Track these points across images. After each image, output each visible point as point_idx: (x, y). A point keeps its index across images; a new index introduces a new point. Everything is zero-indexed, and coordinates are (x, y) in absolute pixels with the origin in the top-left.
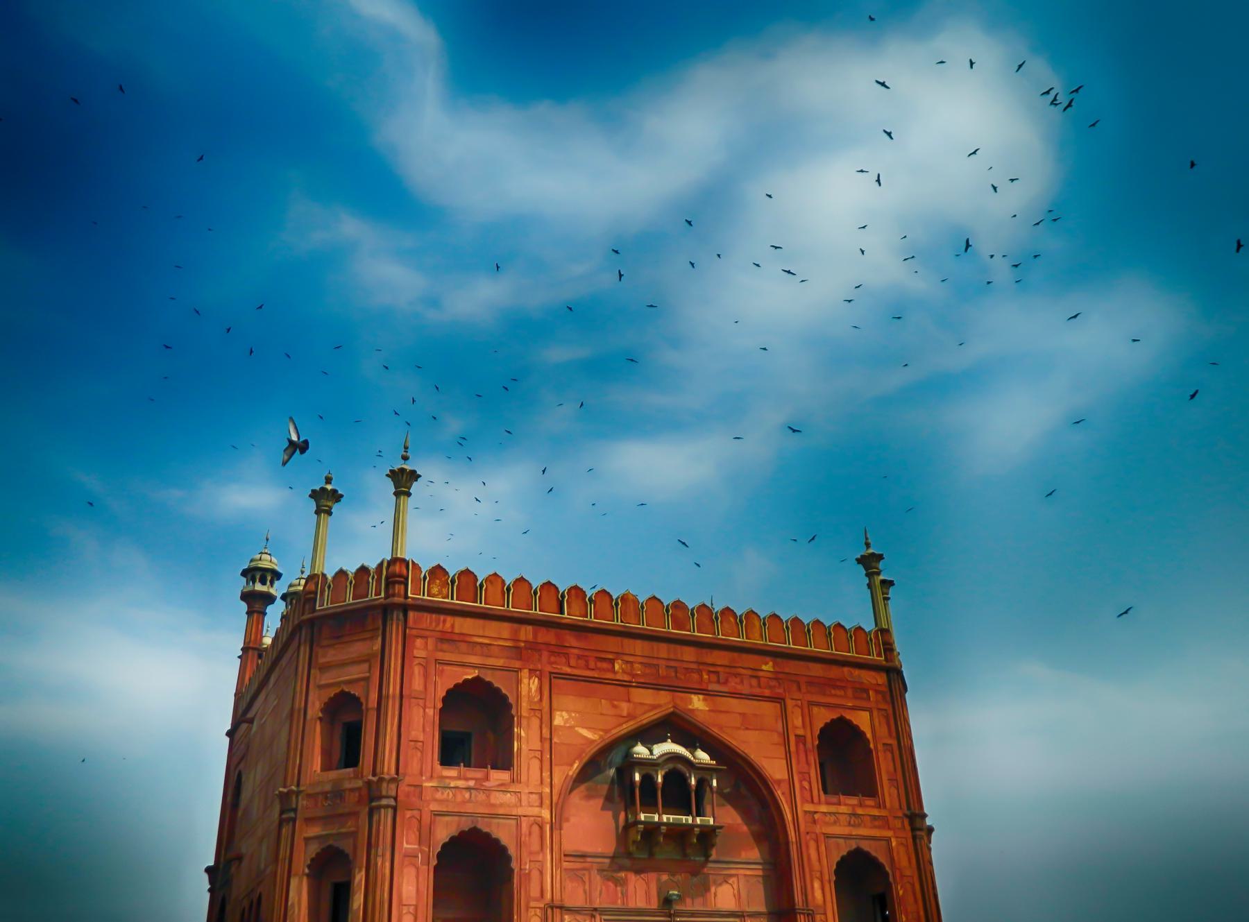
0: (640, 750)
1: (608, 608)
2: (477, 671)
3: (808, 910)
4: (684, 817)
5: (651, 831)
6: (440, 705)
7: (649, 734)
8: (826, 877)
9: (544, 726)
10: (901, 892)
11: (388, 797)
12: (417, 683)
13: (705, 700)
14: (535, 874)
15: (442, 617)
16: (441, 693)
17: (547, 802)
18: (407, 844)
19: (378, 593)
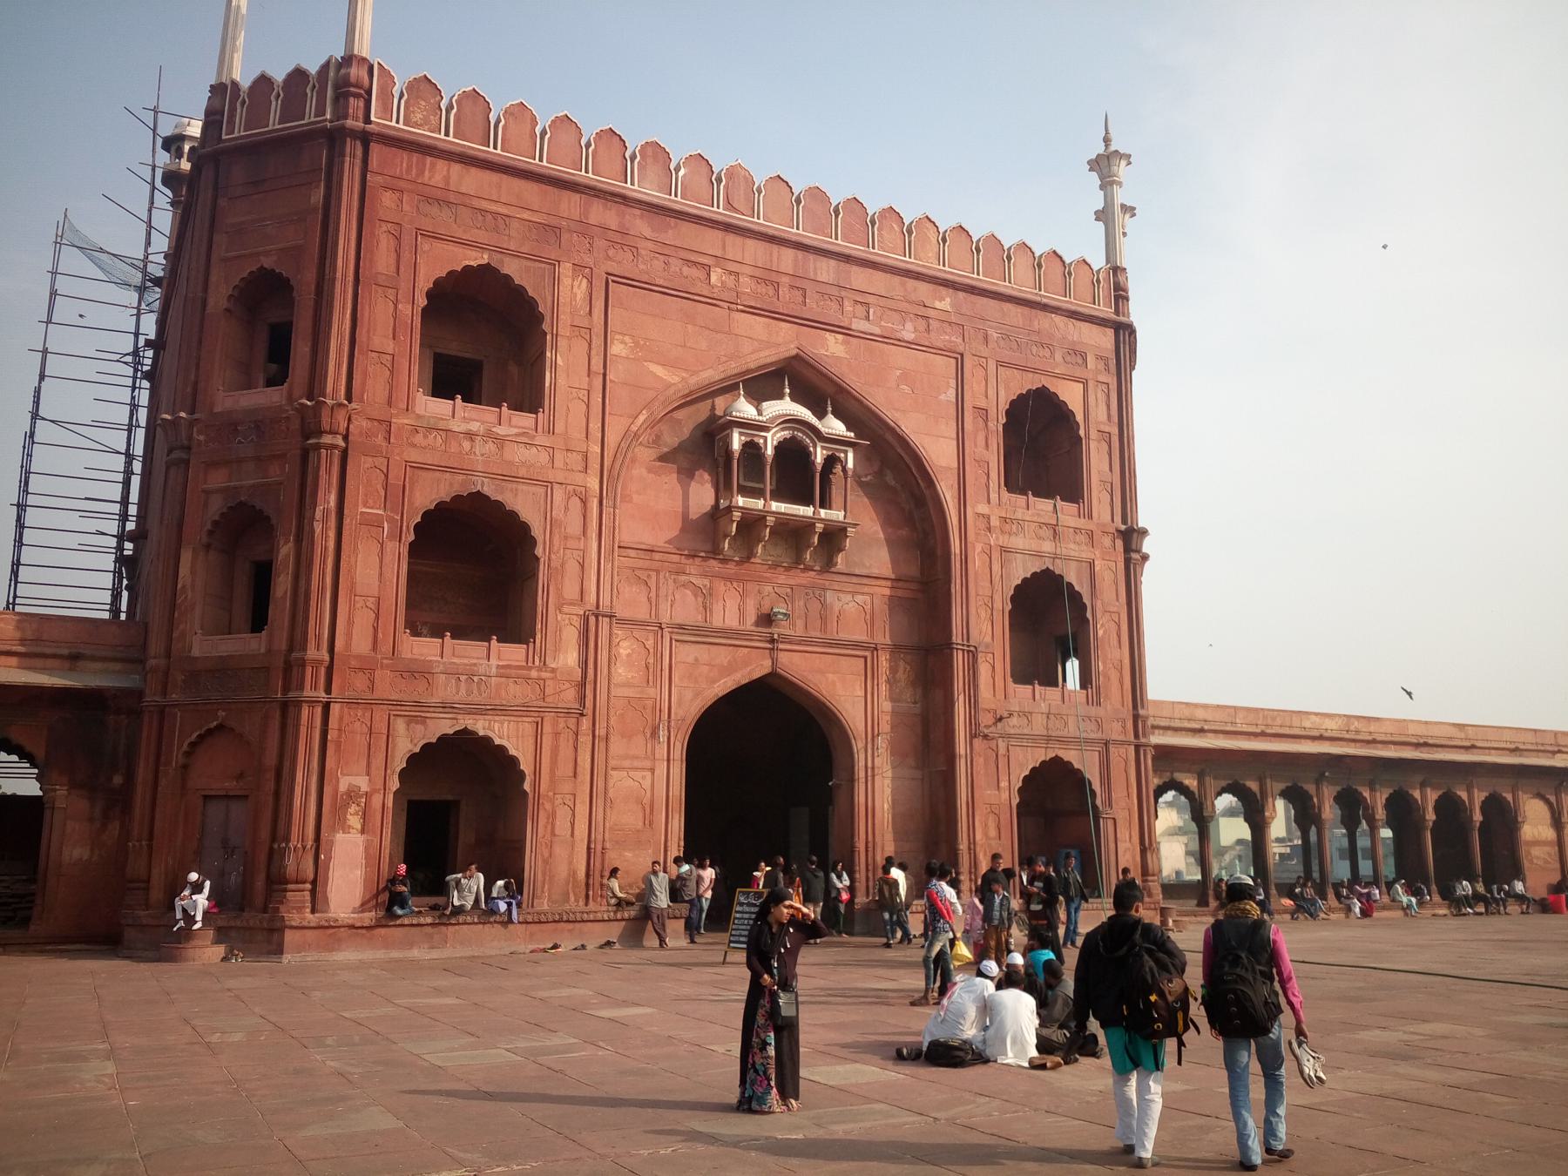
0: (744, 408)
1: (705, 182)
2: (486, 256)
3: (968, 646)
4: (802, 508)
5: (751, 524)
6: (422, 301)
7: (762, 385)
8: (998, 605)
9: (593, 352)
10: (1100, 633)
11: (333, 433)
13: (844, 343)
14: (572, 568)
15: (429, 159)
16: (425, 283)
17: (595, 465)
18: (364, 504)
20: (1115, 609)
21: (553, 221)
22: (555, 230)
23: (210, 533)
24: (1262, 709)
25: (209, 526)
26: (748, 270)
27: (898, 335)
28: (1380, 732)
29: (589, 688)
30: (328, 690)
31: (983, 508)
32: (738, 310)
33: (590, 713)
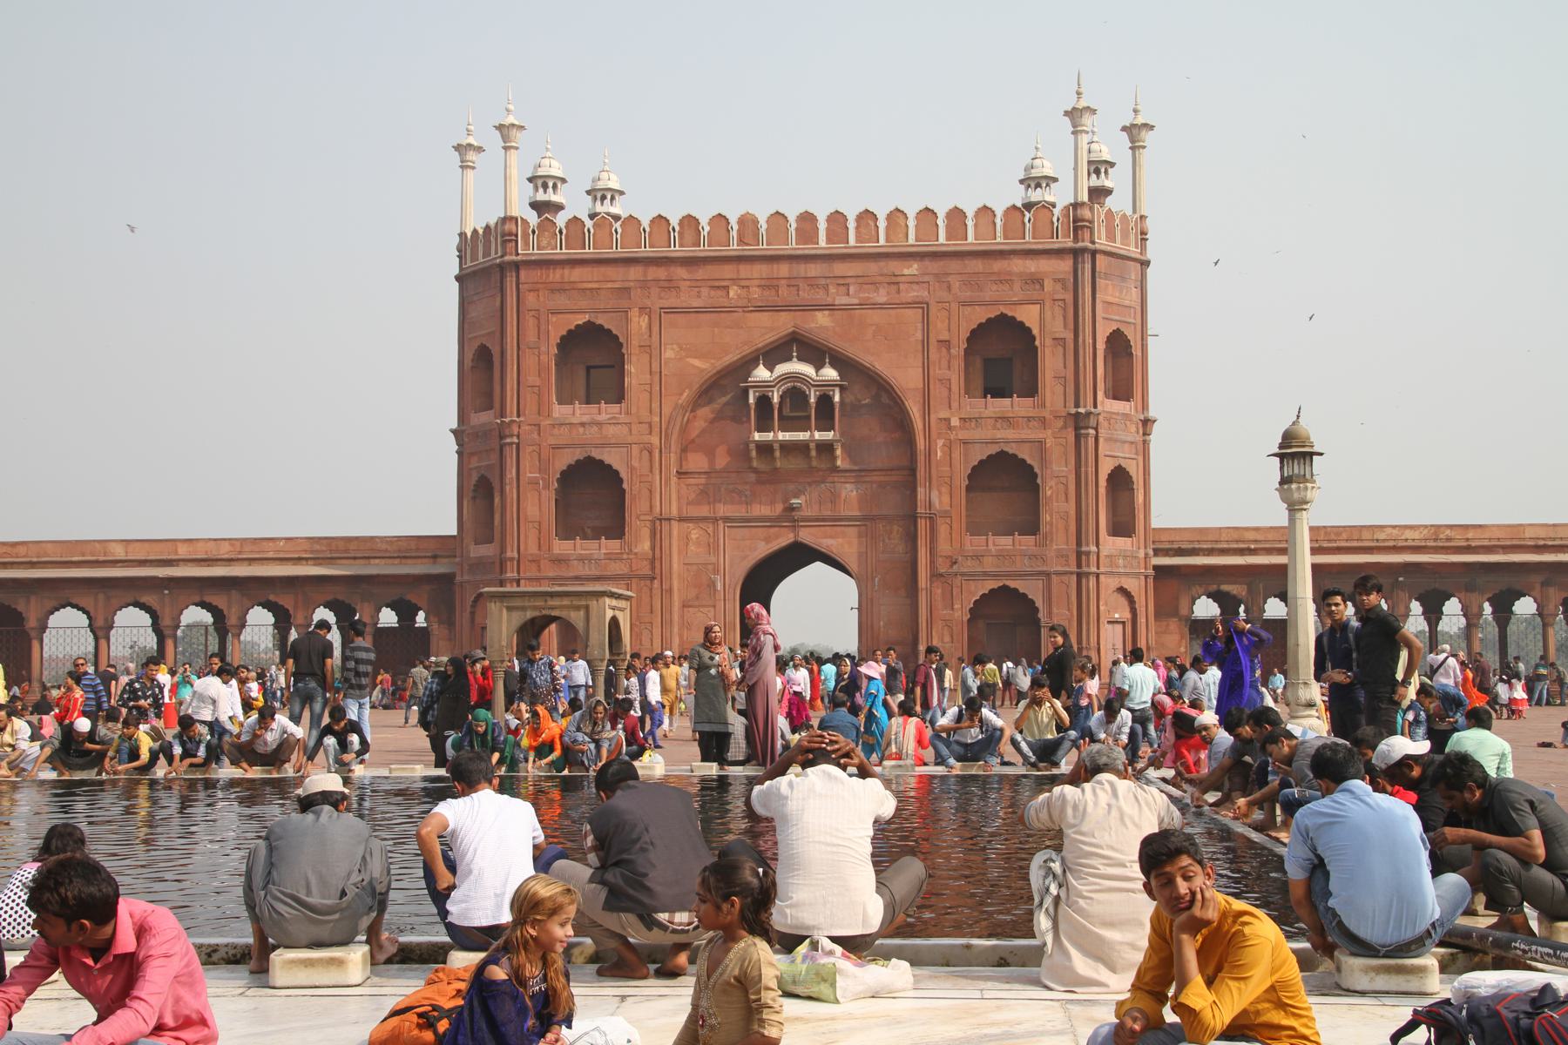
0: (761, 373)
5: (765, 449)
7: (773, 355)
10: (1049, 493)
11: (512, 436)
12: (531, 336)
13: (829, 315)
16: (555, 339)
17: (656, 430)
18: (529, 474)
19: (496, 253)
20: (1064, 474)
21: (627, 285)
22: (627, 290)
23: (474, 491)
24: (1324, 527)
25: (472, 488)
26: (757, 282)
27: (872, 301)
28: (1477, 539)
29: (657, 564)
30: (519, 573)
31: (944, 414)
32: (748, 312)
33: (659, 577)
